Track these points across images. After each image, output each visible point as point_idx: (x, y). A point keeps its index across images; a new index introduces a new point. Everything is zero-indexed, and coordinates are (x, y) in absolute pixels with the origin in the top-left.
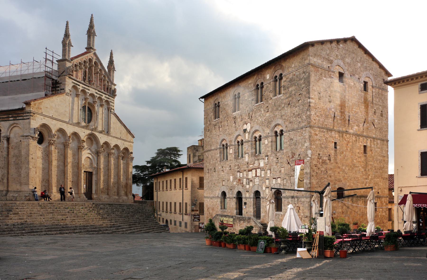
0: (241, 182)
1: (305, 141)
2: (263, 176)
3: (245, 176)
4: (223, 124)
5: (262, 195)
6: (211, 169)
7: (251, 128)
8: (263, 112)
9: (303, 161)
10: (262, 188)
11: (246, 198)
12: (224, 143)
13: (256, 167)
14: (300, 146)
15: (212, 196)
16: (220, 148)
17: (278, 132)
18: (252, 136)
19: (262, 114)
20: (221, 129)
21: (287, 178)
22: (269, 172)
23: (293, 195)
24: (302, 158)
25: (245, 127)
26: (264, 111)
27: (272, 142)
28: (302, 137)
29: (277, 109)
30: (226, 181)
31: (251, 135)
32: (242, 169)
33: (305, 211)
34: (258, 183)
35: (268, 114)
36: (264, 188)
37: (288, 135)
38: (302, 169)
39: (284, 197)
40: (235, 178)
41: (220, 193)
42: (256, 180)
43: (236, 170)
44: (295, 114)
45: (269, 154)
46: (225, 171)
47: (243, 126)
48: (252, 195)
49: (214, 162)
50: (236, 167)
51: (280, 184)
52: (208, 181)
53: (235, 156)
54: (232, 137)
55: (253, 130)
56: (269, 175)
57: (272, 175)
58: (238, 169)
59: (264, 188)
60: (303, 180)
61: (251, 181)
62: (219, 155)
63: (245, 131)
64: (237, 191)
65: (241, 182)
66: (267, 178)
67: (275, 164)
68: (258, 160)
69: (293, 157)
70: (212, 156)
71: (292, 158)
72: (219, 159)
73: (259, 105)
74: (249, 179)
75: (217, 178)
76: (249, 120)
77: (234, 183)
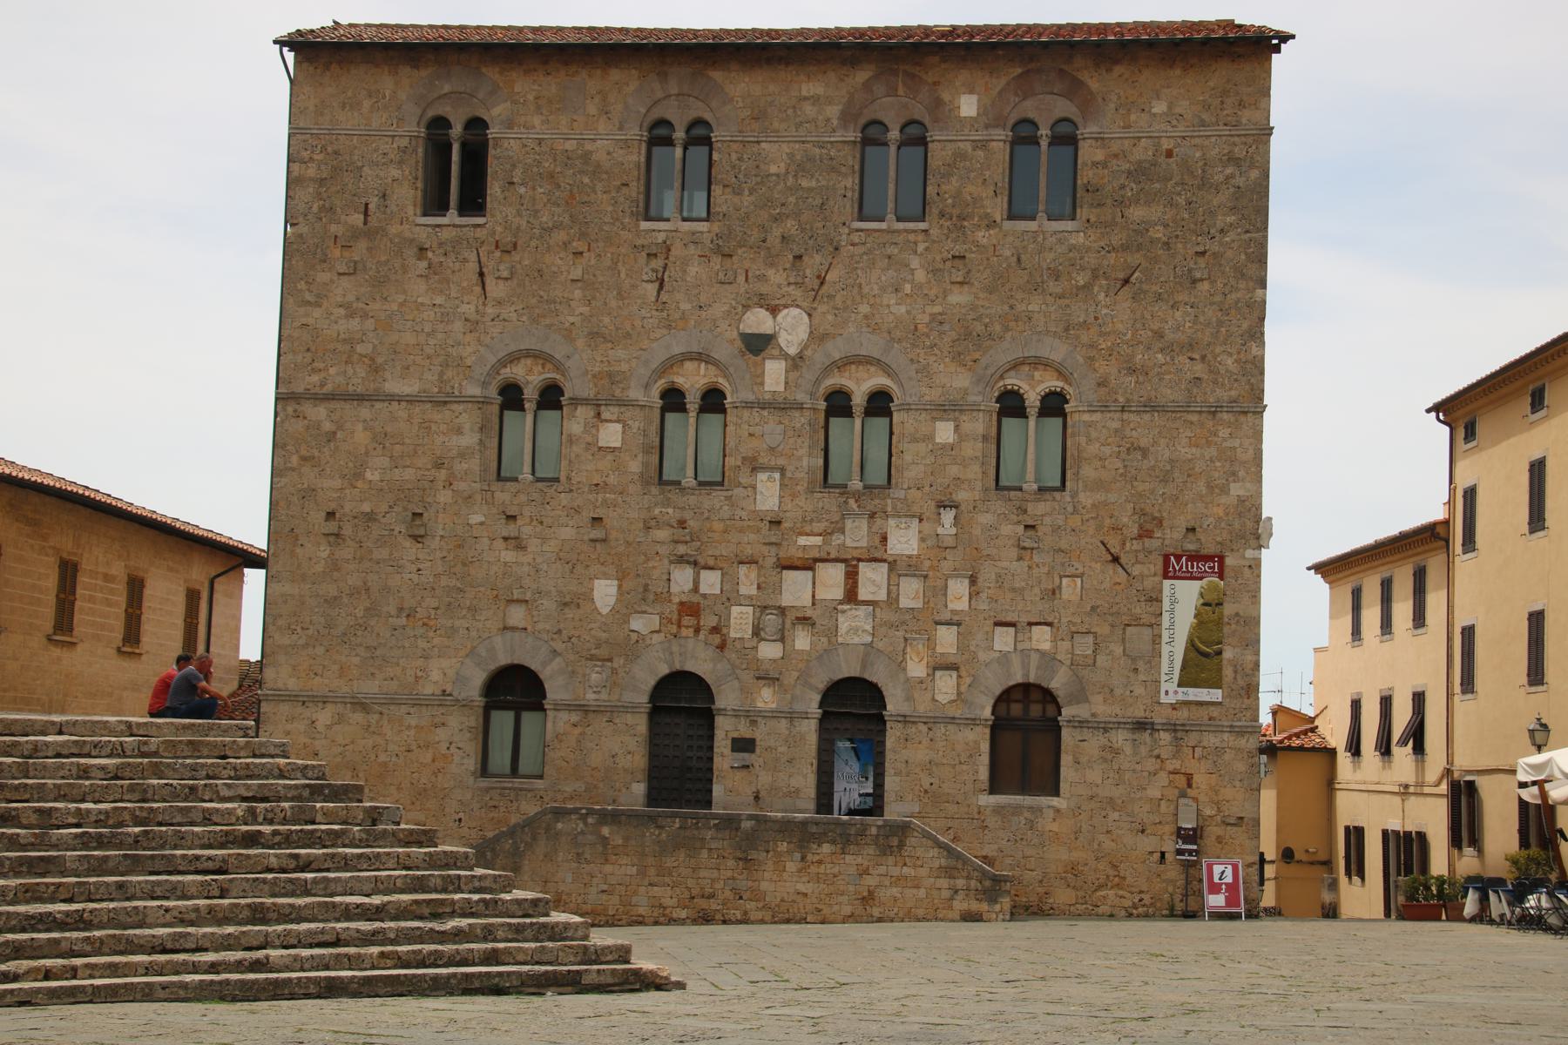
0: (709, 621)
1: (1234, 474)
2: (905, 602)
3: (748, 588)
4: (524, 259)
5: (893, 706)
6: (370, 517)
7: (817, 336)
8: (920, 276)
9: (1221, 559)
10: (902, 666)
11: (752, 717)
12: (532, 379)
13: (856, 554)
14: (1201, 486)
15: (370, 687)
16: (483, 402)
17: (1032, 399)
18: (818, 382)
19: (918, 287)
20: (496, 289)
21: (1104, 630)
22: (958, 590)
23: (1139, 713)
24: (1210, 549)
25: (758, 321)
26: (935, 271)
27: (985, 438)
28: (1213, 451)
29: (1036, 287)
30: (548, 605)
31: (809, 375)
32: (724, 550)
33: (1228, 793)
34: (869, 639)
35: (958, 297)
36: (917, 669)
37: (1116, 425)
38: (1208, 598)
39: (1082, 724)
40: (640, 594)
41: (478, 678)
42: (844, 624)
43: (663, 550)
44: (1170, 336)
45: (962, 496)
46: (533, 545)
47: (735, 315)
48: (818, 697)
49: (409, 474)
50: (662, 534)
51: (1049, 659)
52: (332, 590)
53: (645, 465)
54: (620, 353)
55: (836, 349)
56: (963, 605)
57: (982, 606)
58: (682, 549)
59: (917, 669)
60: (1219, 653)
61: (804, 620)
62: (469, 439)
63: (758, 344)
64: (664, 670)
65: (709, 621)
66: (946, 616)
67: (1014, 553)
68: (872, 516)
69: (1144, 534)
70: (381, 439)
71: (1140, 537)
72: (474, 464)
73: (890, 231)
74: (782, 611)
75: (444, 581)
76: (797, 293)
77: (637, 623)
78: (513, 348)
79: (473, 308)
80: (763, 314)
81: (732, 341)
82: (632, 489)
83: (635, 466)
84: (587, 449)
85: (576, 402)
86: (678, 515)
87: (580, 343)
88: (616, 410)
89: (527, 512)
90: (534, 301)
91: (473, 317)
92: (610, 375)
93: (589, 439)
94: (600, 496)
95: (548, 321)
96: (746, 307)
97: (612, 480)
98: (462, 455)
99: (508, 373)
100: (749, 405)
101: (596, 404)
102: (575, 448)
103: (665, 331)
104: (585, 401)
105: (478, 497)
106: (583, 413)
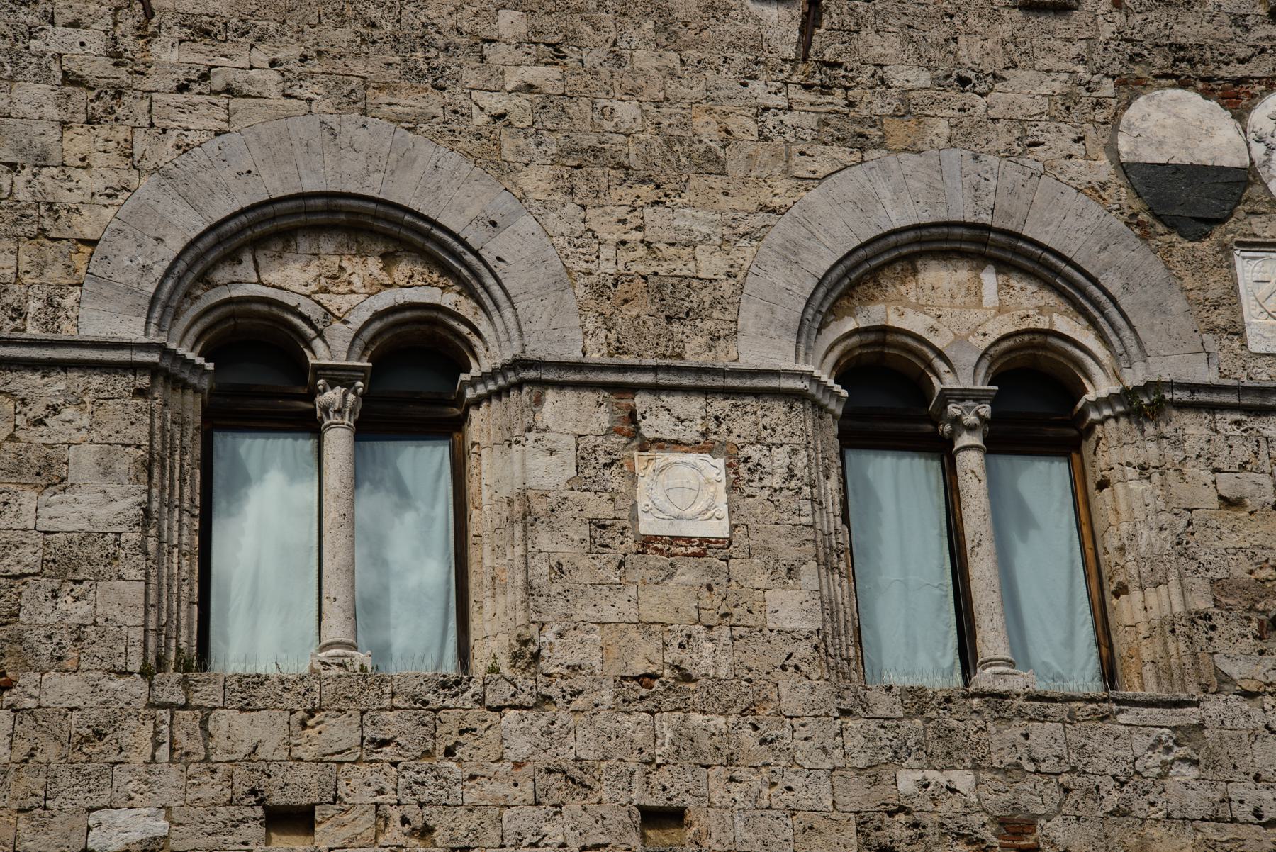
16: (165, 373)
53: (829, 609)
78: (274, 184)
79: (96, 42)
80: (1192, 104)
81: (1096, 191)
82: (791, 694)
83: (792, 609)
84: (597, 547)
85: (529, 376)
86: (997, 803)
87: (535, 181)
88: (695, 406)
89: (359, 786)
90: (343, 36)
91: (98, 68)
92: (657, 288)
93: (600, 508)
94: (666, 724)
95: (406, 102)
96: (1130, 87)
97: (709, 658)
98: (64, 565)
99: (246, 282)
100: (1202, 399)
101: (615, 384)
102: (544, 540)
103: (841, 154)
104: (573, 376)
105: (138, 737)
106: (571, 416)
